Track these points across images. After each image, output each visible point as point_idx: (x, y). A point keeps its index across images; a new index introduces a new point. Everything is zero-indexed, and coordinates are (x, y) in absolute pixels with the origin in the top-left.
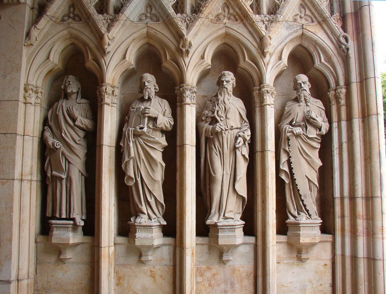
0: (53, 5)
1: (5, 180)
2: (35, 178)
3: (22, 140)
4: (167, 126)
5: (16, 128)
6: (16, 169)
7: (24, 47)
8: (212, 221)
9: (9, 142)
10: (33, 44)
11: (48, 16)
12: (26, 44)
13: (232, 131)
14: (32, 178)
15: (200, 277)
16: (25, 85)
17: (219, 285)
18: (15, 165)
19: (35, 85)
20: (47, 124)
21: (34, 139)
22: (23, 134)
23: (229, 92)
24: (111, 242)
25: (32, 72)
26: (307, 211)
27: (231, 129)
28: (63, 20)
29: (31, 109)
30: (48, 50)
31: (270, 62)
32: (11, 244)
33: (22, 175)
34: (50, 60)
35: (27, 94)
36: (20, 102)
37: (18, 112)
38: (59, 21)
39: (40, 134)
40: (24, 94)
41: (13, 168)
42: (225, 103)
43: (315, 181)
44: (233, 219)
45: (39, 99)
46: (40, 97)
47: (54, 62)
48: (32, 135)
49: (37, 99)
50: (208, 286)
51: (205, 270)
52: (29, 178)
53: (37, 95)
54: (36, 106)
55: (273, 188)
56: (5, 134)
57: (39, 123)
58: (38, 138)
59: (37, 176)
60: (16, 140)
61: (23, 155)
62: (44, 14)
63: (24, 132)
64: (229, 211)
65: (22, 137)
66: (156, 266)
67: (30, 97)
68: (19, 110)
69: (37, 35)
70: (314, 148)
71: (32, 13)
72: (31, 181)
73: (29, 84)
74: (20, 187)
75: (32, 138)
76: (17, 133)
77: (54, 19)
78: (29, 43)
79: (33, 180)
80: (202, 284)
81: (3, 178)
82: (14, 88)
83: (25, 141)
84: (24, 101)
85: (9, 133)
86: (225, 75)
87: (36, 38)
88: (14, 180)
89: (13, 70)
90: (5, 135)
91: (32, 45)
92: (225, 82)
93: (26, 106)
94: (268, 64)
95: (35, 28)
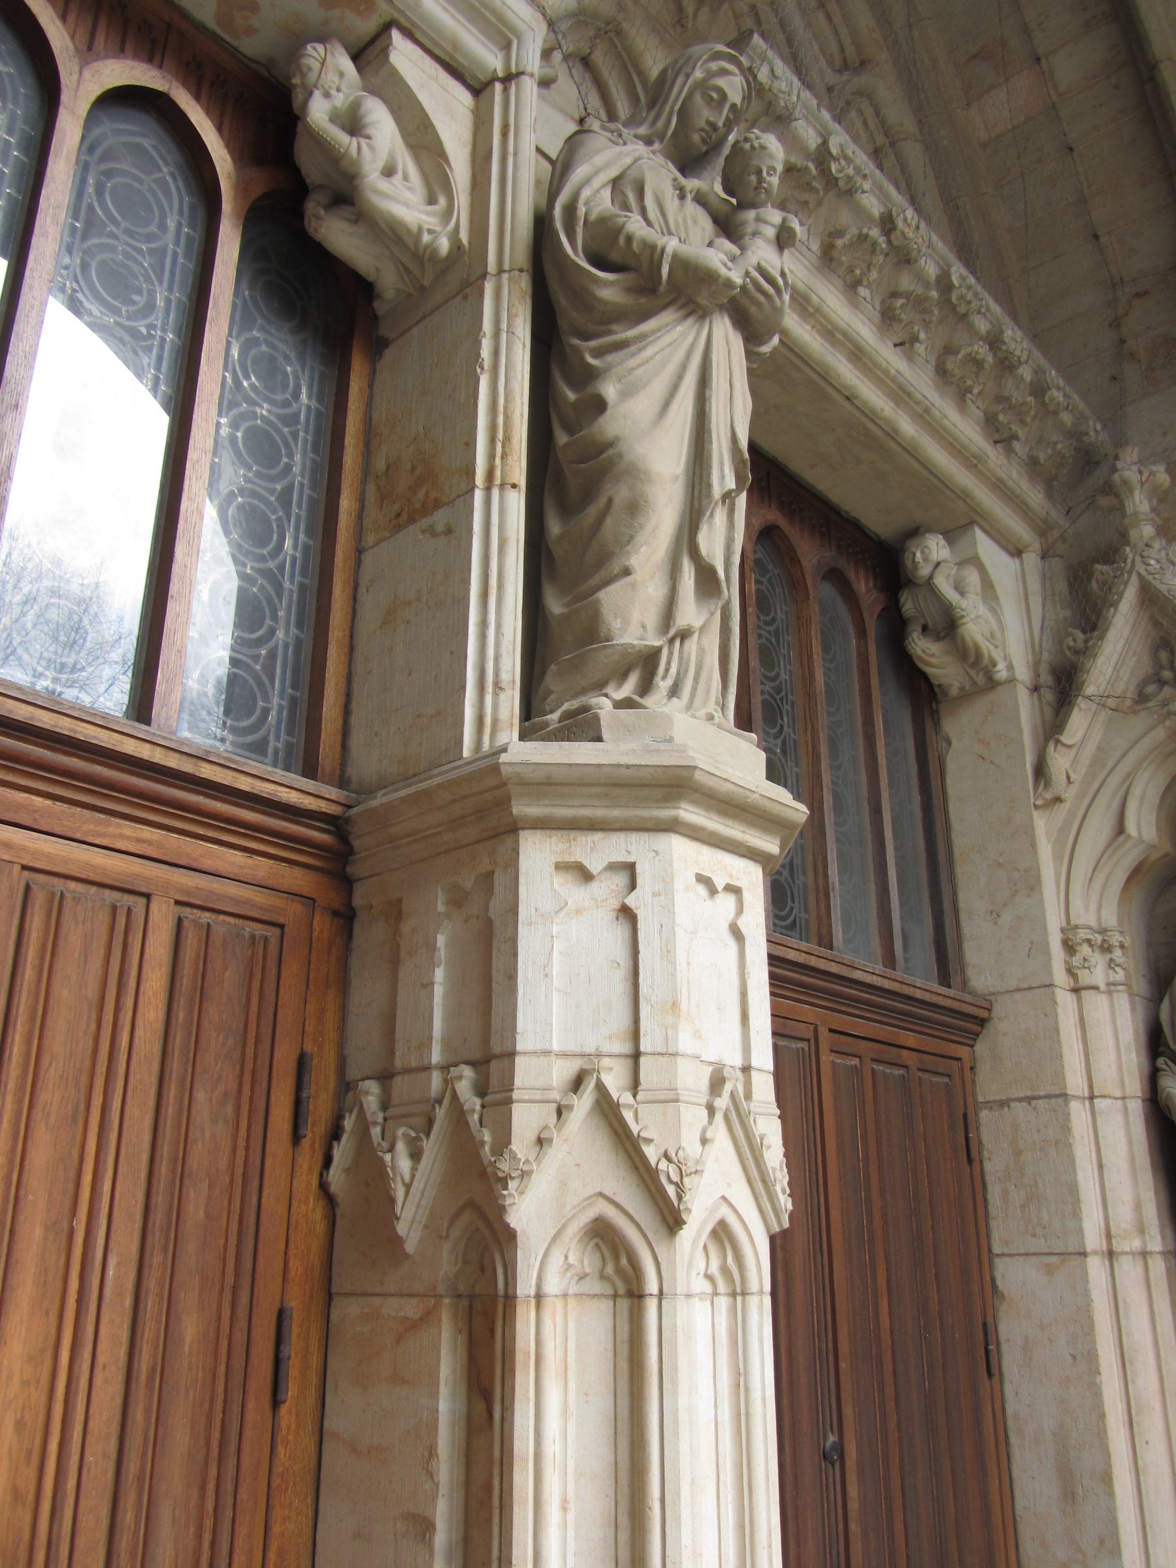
0: (1100, 661)
1: (1054, 1259)
2: (1156, 1244)
3: (1089, 1115)
5: (1059, 1076)
6: (1084, 1217)
7: (1035, 814)
9: (1046, 1127)
10: (1063, 796)
11: (1088, 698)
12: (1039, 802)
14: (1144, 1242)
16: (1063, 930)
18: (1078, 1201)
19: (1093, 924)
20: (1162, 1049)
21: (1129, 1106)
22: (1086, 1094)
25: (1077, 886)
28: (1142, 698)
29: (1098, 1007)
30: (1116, 804)
32: (1111, 1494)
33: (1109, 1236)
34: (1129, 836)
35: (1076, 960)
36: (1057, 991)
37: (1057, 1023)
38: (1128, 702)
39: (1147, 1087)
40: (1065, 961)
41: (1076, 1214)
45: (1118, 969)
46: (1120, 961)
47: (1145, 837)
48: (1118, 1094)
49: (1113, 969)
52: (1136, 1244)
53: (1109, 956)
54: (1115, 995)
56: (1029, 1099)
57: (1133, 1048)
58: (1140, 1101)
59: (1163, 1238)
60: (1067, 1116)
61: (1101, 1167)
62: (1077, 696)
63: (1091, 1087)
65: (1087, 1103)
67: (1089, 968)
68: (1061, 1017)
69: (1068, 767)
71: (1037, 703)
72: (1144, 1254)
73: (1076, 927)
74: (1109, 1279)
75: (1119, 1103)
76: (1069, 1092)
77: (1111, 703)
78: (1048, 796)
79: (1151, 1253)
81: (1048, 1250)
82: (1029, 946)
83: (1097, 1115)
84: (1072, 984)
85: (1043, 1093)
87: (1068, 777)
88: (1084, 1254)
89: (1017, 891)
90: (1030, 1103)
91: (1058, 800)
93: (1079, 1000)
95: (1059, 745)
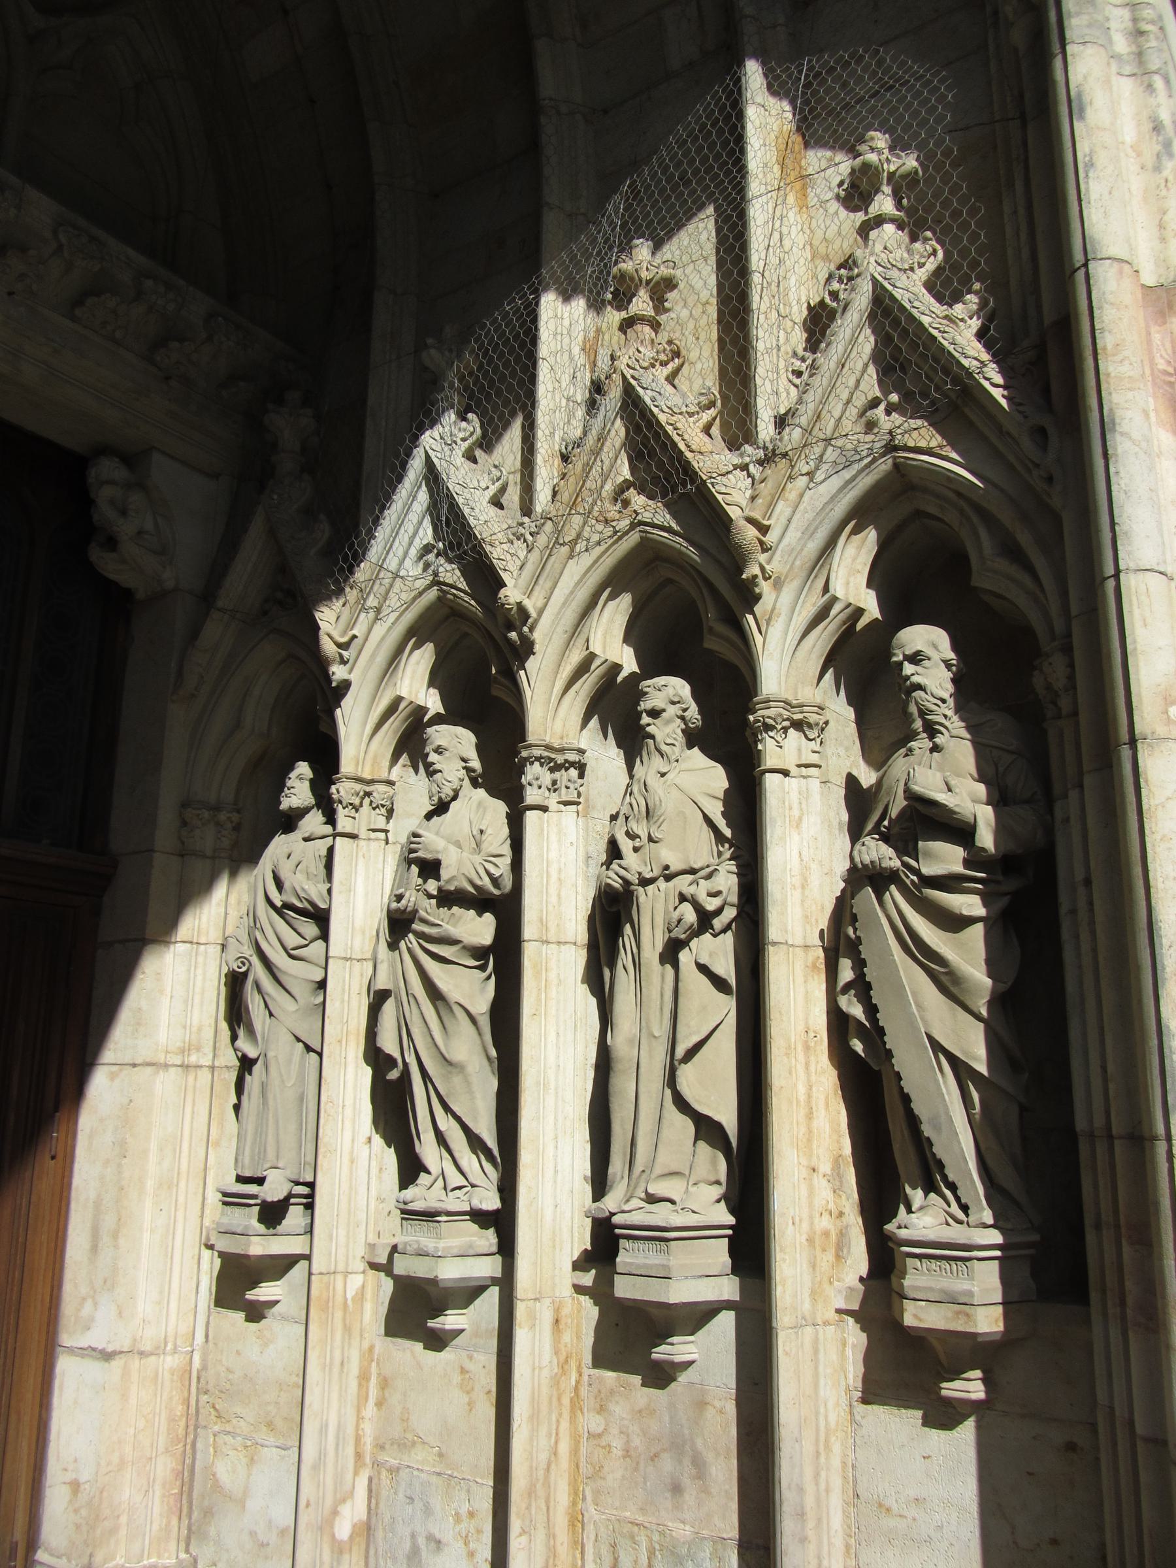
4: (479, 882)
8: (603, 1207)
13: (671, 884)
15: (598, 1413)
17: (656, 1459)
21: (209, 951)
23: (664, 748)
24: (354, 1257)
26: (953, 1187)
27: (668, 878)
31: (776, 611)
42: (647, 791)
43: (976, 1059)
44: (673, 1202)
45: (223, 839)
50: (620, 1453)
51: (612, 1392)
55: (811, 1086)
64: (666, 1171)
66: (475, 1355)
70: (954, 923)
80: (604, 1444)
86: (646, 693)
92: (644, 715)
94: (768, 622)
